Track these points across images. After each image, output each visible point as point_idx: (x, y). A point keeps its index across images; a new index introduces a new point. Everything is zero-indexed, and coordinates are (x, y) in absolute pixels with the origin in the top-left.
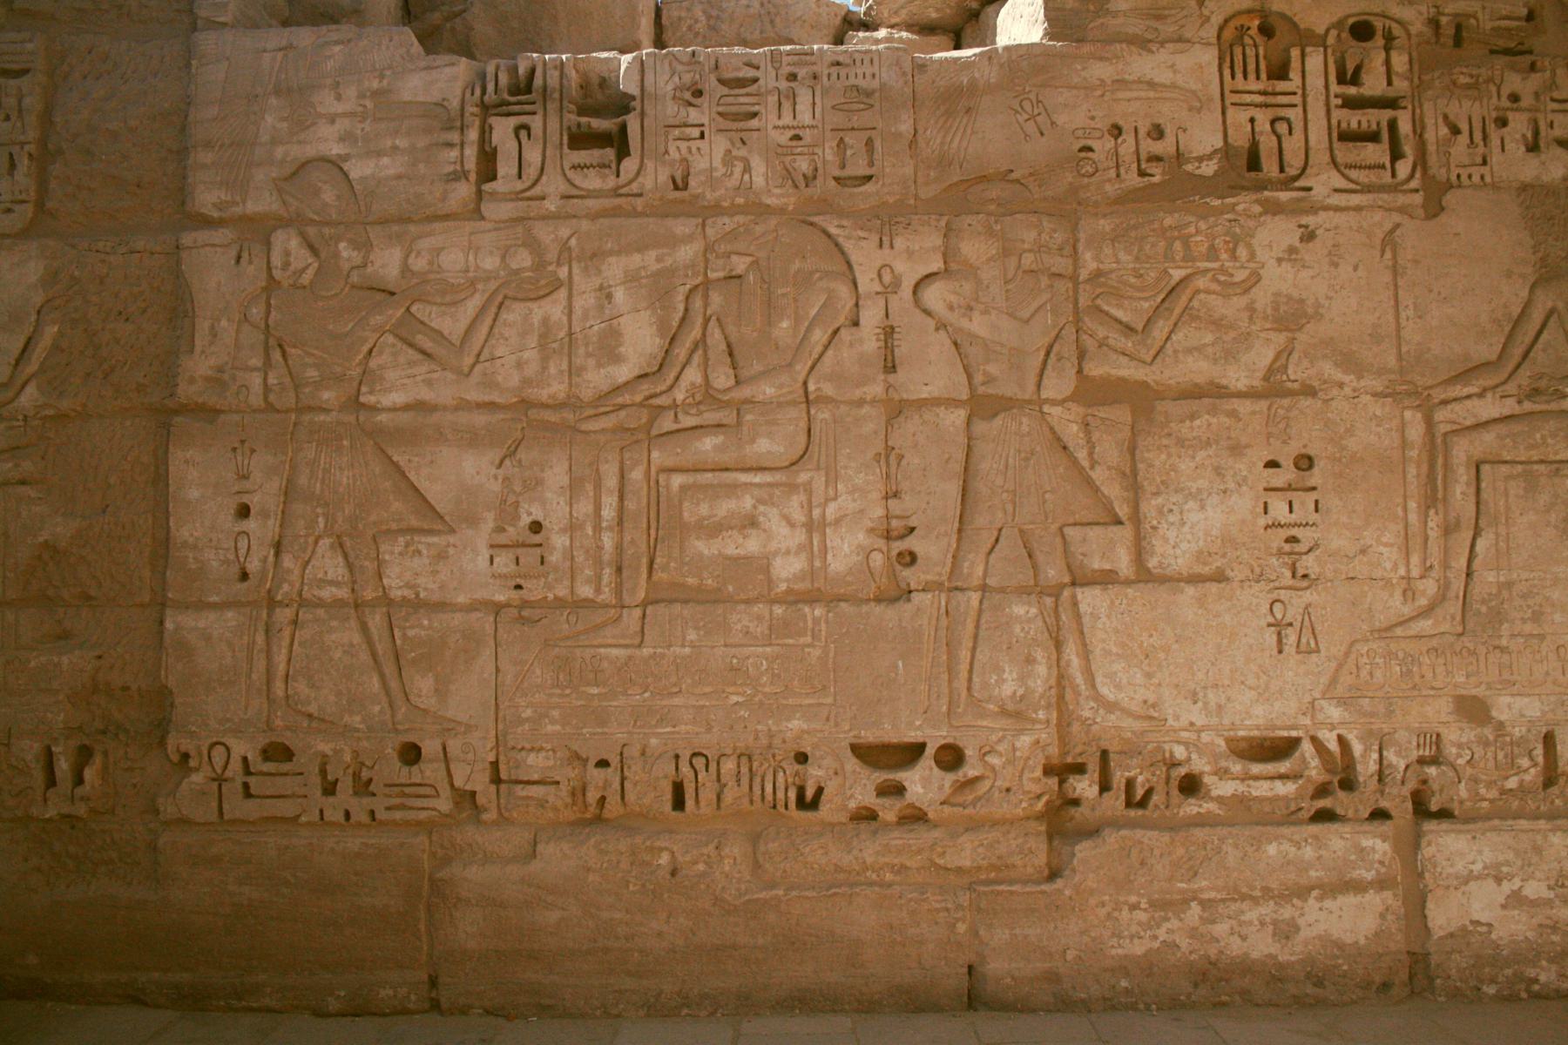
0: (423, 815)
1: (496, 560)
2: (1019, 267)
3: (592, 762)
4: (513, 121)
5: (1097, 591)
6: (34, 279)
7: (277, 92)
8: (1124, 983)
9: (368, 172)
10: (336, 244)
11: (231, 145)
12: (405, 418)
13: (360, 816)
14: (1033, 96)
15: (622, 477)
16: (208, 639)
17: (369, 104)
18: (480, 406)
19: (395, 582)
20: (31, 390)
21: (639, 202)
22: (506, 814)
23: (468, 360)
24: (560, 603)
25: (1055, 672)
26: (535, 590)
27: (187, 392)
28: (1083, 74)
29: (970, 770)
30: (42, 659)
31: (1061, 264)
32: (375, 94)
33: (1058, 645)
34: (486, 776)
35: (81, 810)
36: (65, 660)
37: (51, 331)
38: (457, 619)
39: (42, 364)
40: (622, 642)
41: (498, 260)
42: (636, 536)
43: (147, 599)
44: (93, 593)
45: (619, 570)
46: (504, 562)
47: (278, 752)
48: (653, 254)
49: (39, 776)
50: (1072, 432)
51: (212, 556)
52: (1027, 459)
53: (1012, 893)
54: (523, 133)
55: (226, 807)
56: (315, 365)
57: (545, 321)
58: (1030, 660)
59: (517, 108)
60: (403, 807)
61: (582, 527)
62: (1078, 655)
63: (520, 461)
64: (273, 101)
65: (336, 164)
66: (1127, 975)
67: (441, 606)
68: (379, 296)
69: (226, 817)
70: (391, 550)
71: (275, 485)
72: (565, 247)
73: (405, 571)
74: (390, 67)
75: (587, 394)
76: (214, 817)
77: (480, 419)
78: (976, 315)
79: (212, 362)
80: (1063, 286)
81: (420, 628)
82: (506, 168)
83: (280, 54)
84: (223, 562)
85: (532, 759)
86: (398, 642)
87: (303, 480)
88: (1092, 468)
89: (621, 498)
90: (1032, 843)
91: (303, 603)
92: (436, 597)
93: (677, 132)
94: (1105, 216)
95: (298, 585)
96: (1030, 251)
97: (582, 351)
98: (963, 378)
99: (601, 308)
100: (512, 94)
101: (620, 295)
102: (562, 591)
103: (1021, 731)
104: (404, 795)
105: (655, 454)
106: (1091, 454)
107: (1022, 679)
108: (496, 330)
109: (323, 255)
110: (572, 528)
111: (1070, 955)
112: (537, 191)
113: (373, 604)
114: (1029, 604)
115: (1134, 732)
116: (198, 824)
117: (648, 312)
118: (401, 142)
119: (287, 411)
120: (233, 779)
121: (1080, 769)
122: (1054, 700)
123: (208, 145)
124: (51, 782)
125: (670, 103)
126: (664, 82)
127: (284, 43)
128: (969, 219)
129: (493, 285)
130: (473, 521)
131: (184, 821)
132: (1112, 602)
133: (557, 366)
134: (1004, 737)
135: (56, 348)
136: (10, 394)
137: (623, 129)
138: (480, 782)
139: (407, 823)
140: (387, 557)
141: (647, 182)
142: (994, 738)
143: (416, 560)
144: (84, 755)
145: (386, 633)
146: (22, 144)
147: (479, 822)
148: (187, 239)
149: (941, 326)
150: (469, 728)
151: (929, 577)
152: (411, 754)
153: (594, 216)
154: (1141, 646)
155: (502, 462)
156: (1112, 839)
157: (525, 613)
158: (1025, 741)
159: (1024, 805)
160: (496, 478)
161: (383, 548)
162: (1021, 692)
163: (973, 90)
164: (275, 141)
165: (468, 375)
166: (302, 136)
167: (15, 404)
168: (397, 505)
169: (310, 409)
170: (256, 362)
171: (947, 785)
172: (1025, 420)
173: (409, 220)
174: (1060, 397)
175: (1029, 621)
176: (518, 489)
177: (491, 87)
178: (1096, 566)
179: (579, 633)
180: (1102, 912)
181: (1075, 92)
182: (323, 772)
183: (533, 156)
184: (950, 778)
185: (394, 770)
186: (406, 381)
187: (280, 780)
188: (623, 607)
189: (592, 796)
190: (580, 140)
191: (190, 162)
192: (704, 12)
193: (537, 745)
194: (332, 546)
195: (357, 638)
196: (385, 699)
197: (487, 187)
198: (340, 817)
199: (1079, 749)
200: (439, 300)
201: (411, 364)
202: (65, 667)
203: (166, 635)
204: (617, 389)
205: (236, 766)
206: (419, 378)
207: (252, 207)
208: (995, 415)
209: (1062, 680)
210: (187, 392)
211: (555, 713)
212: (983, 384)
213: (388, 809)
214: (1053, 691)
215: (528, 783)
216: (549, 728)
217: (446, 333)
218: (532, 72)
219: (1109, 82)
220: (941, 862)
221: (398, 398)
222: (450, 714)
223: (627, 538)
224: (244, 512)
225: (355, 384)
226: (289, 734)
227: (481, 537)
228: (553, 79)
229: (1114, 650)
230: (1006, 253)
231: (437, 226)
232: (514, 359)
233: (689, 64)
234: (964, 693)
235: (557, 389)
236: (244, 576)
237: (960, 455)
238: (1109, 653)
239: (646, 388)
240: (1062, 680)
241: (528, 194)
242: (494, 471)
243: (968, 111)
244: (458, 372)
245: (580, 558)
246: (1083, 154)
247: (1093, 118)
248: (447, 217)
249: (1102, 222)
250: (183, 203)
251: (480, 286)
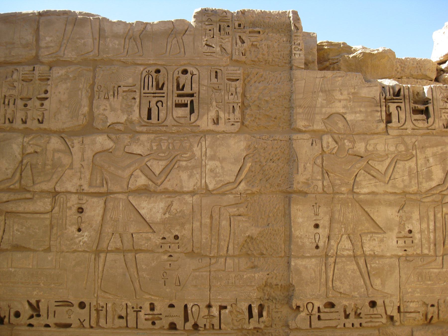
0: (377, 324)
1: (398, 242)
3: (429, 305)
4: (396, 105)
6: (242, 148)
7: (322, 91)
9: (353, 118)
10: (344, 141)
11: (307, 107)
12: (369, 197)
13: (357, 325)
15: (435, 216)
16: (306, 268)
17: (351, 97)
18: (391, 193)
19: (367, 250)
20: (243, 184)
21: (434, 131)
22: (403, 323)
23: (387, 179)
24: (418, 255)
26: (410, 251)
27: (296, 186)
30: (248, 275)
32: (353, 94)
34: (397, 311)
35: (262, 326)
36: (257, 275)
37: (249, 165)
38: (387, 261)
39: (245, 176)
40: (437, 267)
41: (394, 148)
42: (439, 234)
43: (283, 254)
44: (265, 252)
45: (435, 245)
46: (401, 242)
47: (332, 305)
48: (440, 148)
49: (247, 314)
51: (307, 241)
54: (399, 109)
55: (312, 323)
56: (339, 180)
57: (410, 167)
59: (397, 101)
60: (371, 322)
61: (424, 231)
63: (405, 211)
64: (321, 94)
65: (342, 116)
67: (382, 257)
68: (358, 158)
69: (313, 327)
70: (366, 239)
71: (327, 218)
72: (414, 144)
73: (370, 246)
74: (357, 85)
75: (423, 190)
76: (308, 327)
77: (392, 198)
79: (305, 177)
81: (374, 264)
82: (394, 119)
83: (322, 79)
84: (311, 243)
85: (412, 305)
86: (369, 268)
87: (337, 216)
89: (435, 223)
91: (337, 256)
92: (380, 254)
93: (444, 111)
95: (336, 250)
97: (421, 177)
99: (426, 164)
100: (394, 96)
101: (431, 160)
102: (419, 252)
104: (371, 317)
105: (444, 209)
108: (395, 170)
109: (339, 144)
110: (421, 232)
112: (404, 127)
113: (360, 256)
116: (302, 330)
117: (440, 166)
118: (363, 110)
119: (330, 194)
120: (315, 314)
123: (300, 106)
124: (251, 315)
125: (441, 101)
126: (439, 96)
127: (323, 76)
129: (393, 156)
130: (391, 230)
131: (297, 329)
133: (414, 181)
135: (250, 170)
136: (236, 185)
137: (427, 108)
138: (395, 313)
139: (371, 327)
140: (365, 241)
141: (436, 125)
143: (374, 242)
144: (261, 307)
145: (365, 266)
146: (237, 103)
147: (394, 325)
148: (294, 137)
150: (391, 296)
152: (373, 304)
153: (422, 135)
155: (399, 211)
157: (408, 259)
160: (397, 216)
161: (363, 238)
164: (322, 107)
165: (388, 183)
166: (330, 106)
167: (237, 189)
168: (367, 225)
169: (338, 193)
170: (319, 177)
173: (366, 134)
176: (404, 220)
177: (388, 94)
179: (424, 265)
182: (345, 311)
183: (402, 116)
185: (367, 309)
186: (368, 185)
187: (331, 314)
188: (436, 256)
189: (429, 317)
190: (416, 111)
191: (295, 111)
192: (400, 65)
193: (413, 301)
194: (347, 237)
195: (356, 267)
196: (365, 287)
197: (389, 125)
198: (351, 326)
200: (377, 160)
201: (370, 180)
202: (256, 278)
203: (292, 267)
204: (431, 189)
205: (316, 310)
206: (372, 184)
207: (316, 127)
210: (296, 186)
211: (418, 290)
213: (366, 322)
215: (411, 312)
216: (417, 295)
217: (380, 170)
218: (400, 90)
221: (365, 190)
222: (386, 291)
223: (437, 235)
224: (317, 226)
225: (352, 185)
226: (334, 299)
227: (394, 235)
228: (407, 93)
231: (376, 136)
232: (401, 179)
233: (445, 90)
235: (414, 188)
236: (317, 247)
239: (440, 189)
241: (402, 128)
242: (397, 214)
244: (385, 183)
245: (424, 241)
248: (377, 134)
250: (290, 125)
251: (390, 156)
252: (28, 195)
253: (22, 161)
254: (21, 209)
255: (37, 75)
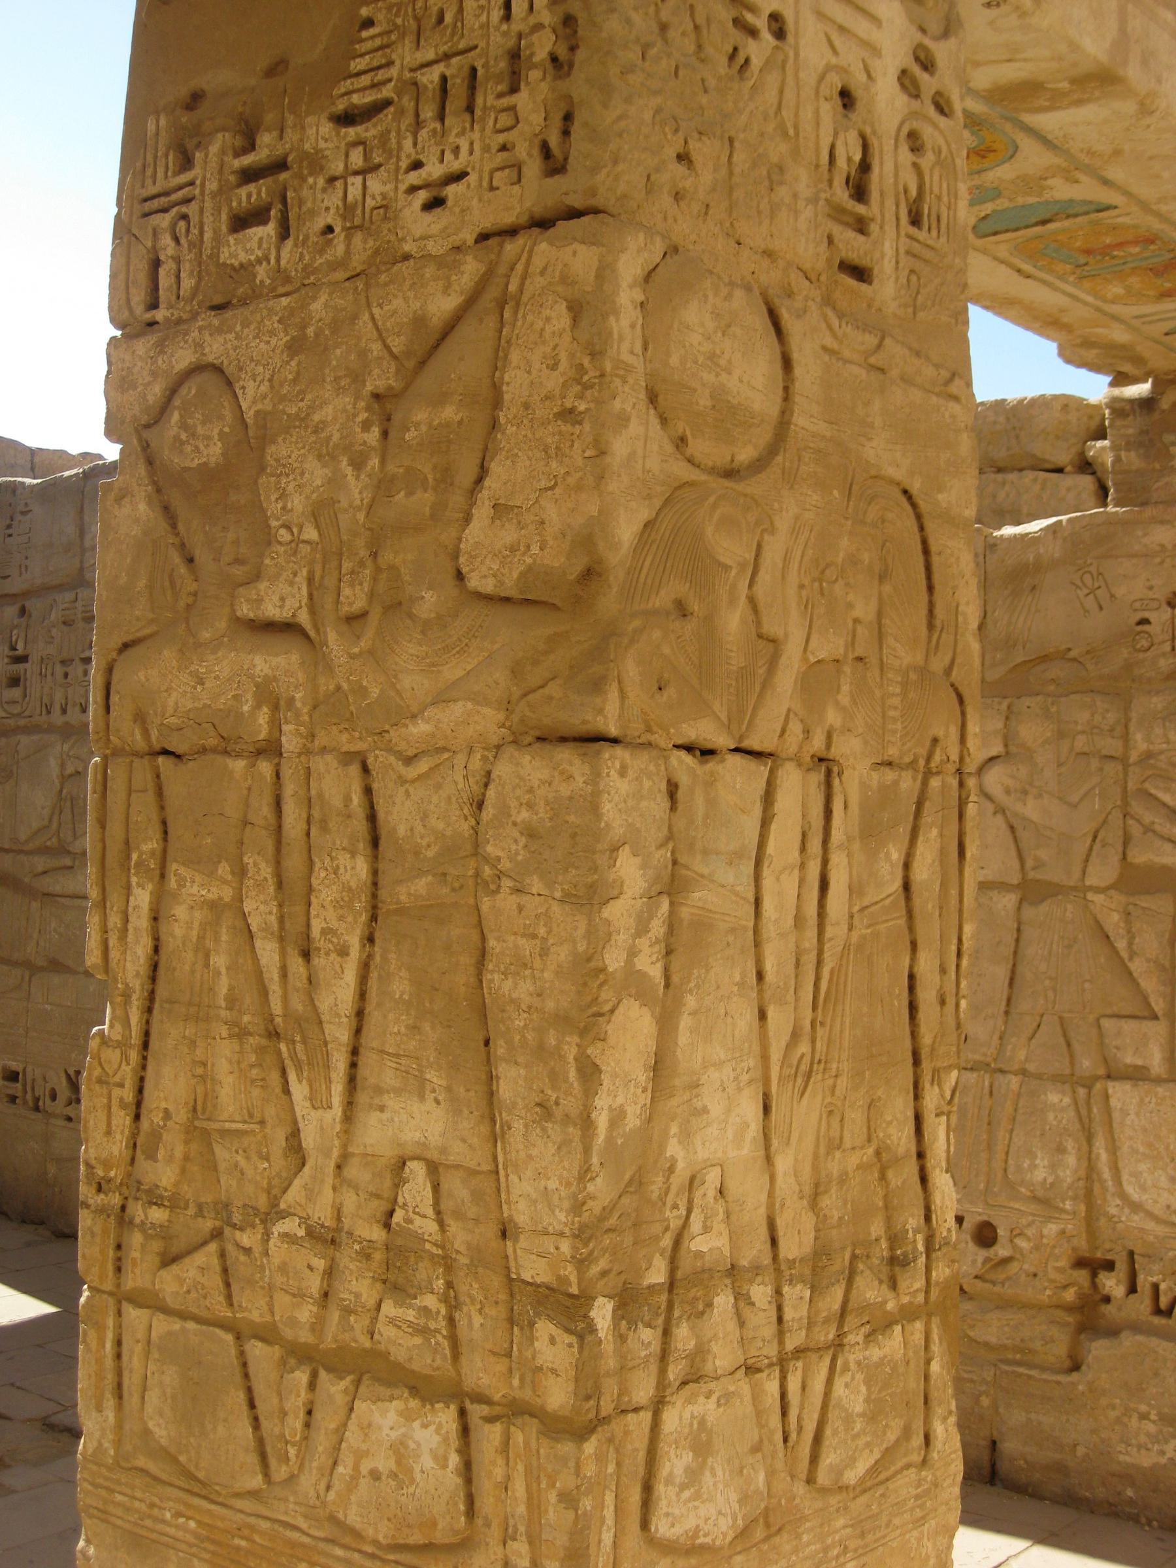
2: (1072, 749)
5: (1127, 1086)
8: (1130, 1493)
14: (1093, 569)
25: (1085, 1164)
28: (1145, 540)
29: (1001, 1250)
31: (1112, 746)
33: (1090, 1139)
50: (1113, 921)
52: (1069, 947)
53: (1030, 1377)
58: (1061, 1150)
62: (1106, 1149)
66: (1133, 1484)
78: (1031, 802)
80: (1111, 768)
88: (1131, 959)
90: (1055, 1332)
94: (1157, 693)
96: (1083, 732)
98: (1016, 864)
103: (1050, 1219)
106: (1130, 944)
107: (1053, 1167)
111: (1081, 1451)
114: (1063, 1093)
115: (1156, 1237)
121: (1110, 1266)
122: (1082, 1192)
128: (1027, 701)
132: (1142, 1100)
134: (1033, 1222)
142: (1024, 1221)
149: (1000, 810)
151: (977, 1057)
154: (1167, 1148)
156: (1128, 1340)
158: (1052, 1229)
159: (1048, 1292)
162: (1050, 1180)
163: (1038, 567)
171: (980, 1260)
172: (1069, 906)
174: (1103, 885)
175: (1062, 1110)
178: (1129, 1060)
180: (1113, 1414)
181: (1135, 561)
184: (982, 1254)
199: (1108, 1246)
208: (1042, 901)
209: (1090, 1172)
212: (1033, 869)
214: (1081, 1184)
219: (1169, 547)
220: (972, 1334)
229: (1141, 1149)
230: (1061, 735)
234: (1000, 1175)
237: (1010, 939)
238: (1137, 1152)
240: (1090, 1172)
243: (1034, 588)
246: (1140, 628)
247: (1151, 588)
249: (1155, 700)
252: (68, 861)
253: (61, 791)
254: (58, 889)
255: (80, 609)
